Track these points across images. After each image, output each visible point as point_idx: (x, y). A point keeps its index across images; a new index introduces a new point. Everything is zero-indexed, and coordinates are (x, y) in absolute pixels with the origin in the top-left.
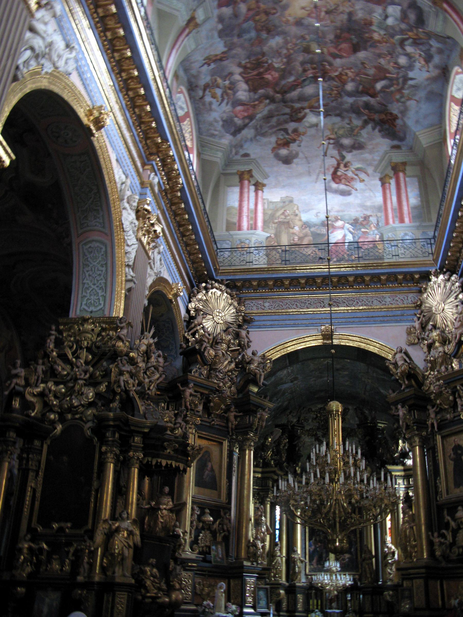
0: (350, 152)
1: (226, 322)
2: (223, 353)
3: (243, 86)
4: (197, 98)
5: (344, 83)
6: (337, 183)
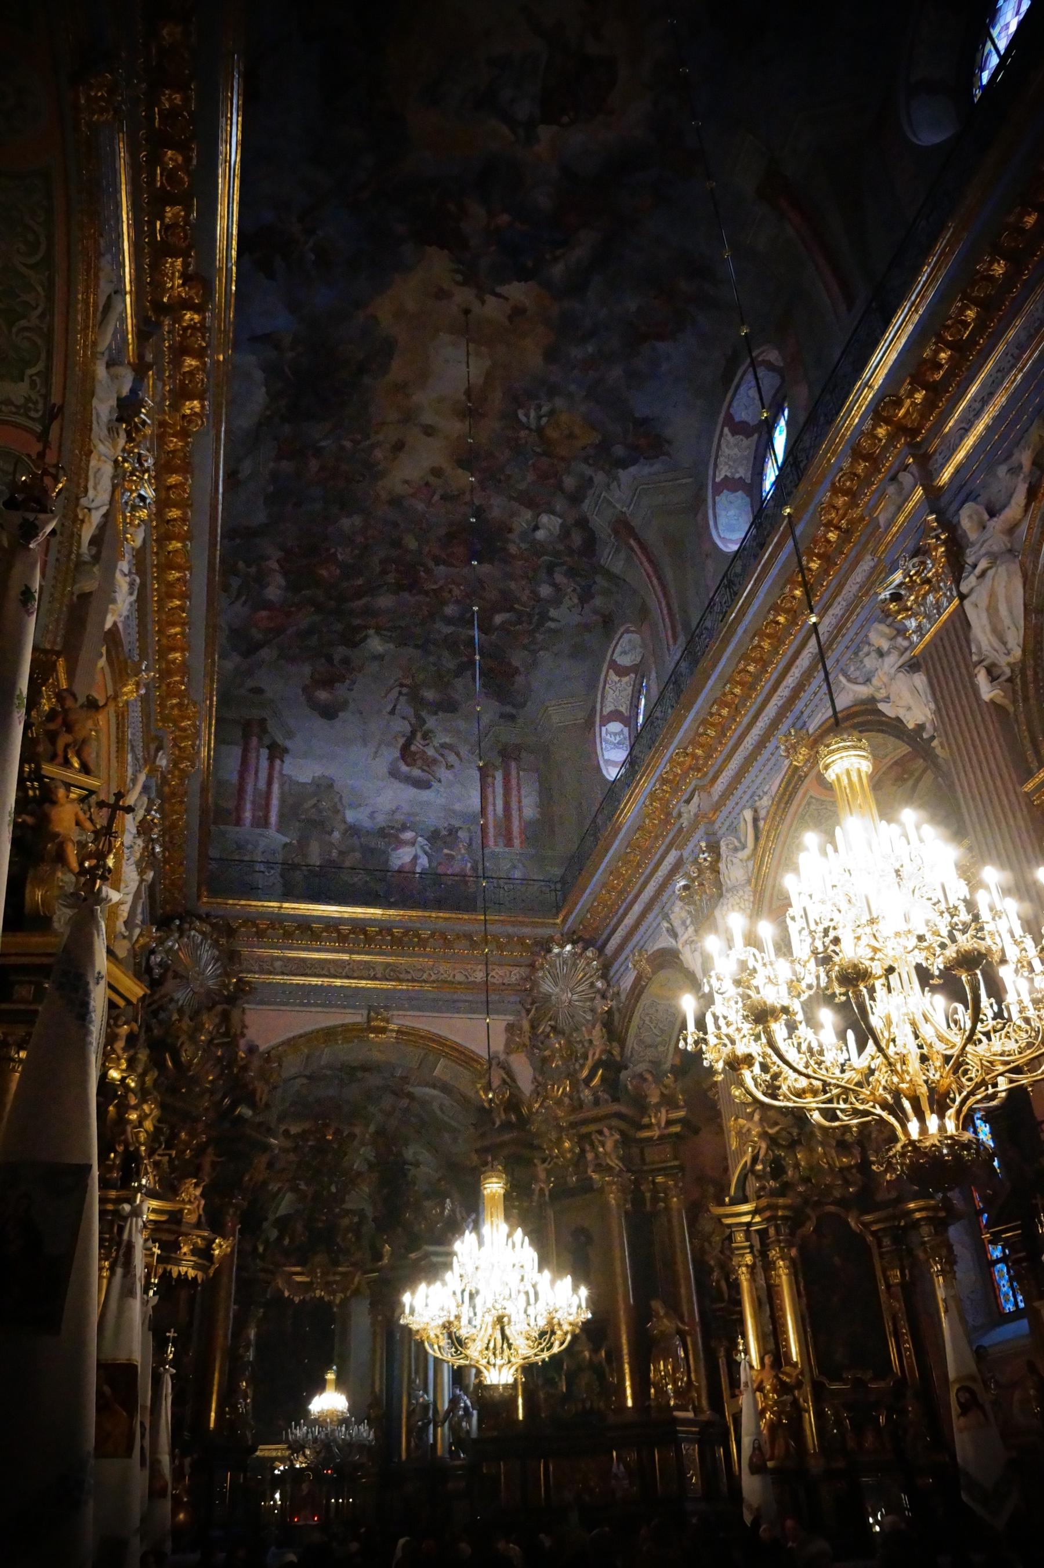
0: (436, 714)
1: (209, 992)
3: (280, 580)
5: (444, 603)
6: (408, 765)
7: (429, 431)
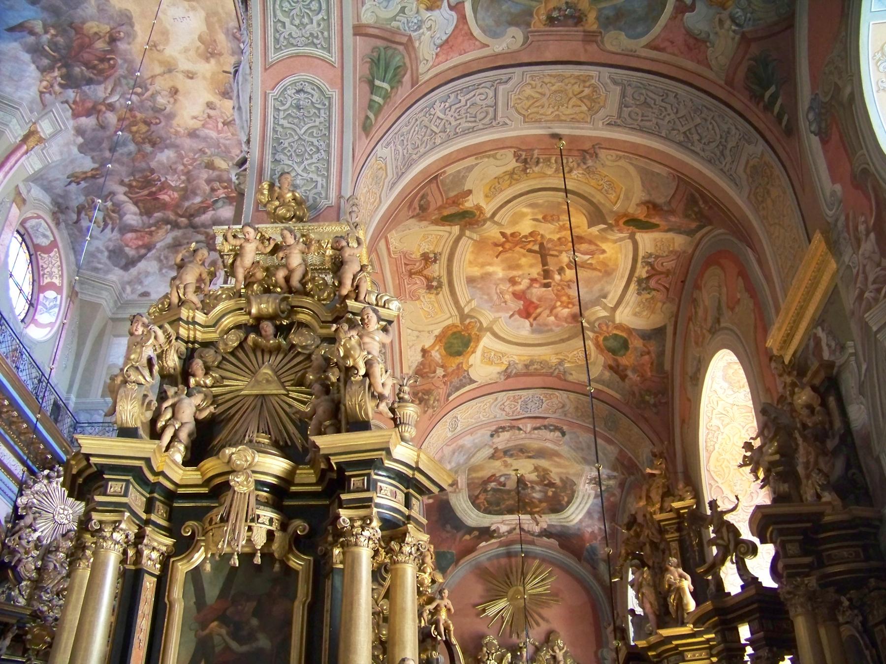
2: (55, 566)
3: (131, 208)
7: (190, 76)
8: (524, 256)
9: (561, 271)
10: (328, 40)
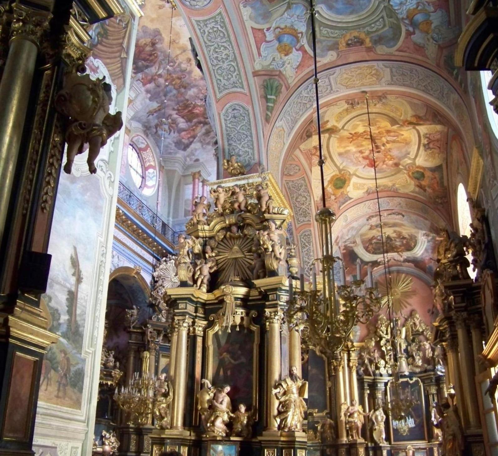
4: (153, 133)
8: (364, 141)
9: (384, 145)
10: (242, 83)
